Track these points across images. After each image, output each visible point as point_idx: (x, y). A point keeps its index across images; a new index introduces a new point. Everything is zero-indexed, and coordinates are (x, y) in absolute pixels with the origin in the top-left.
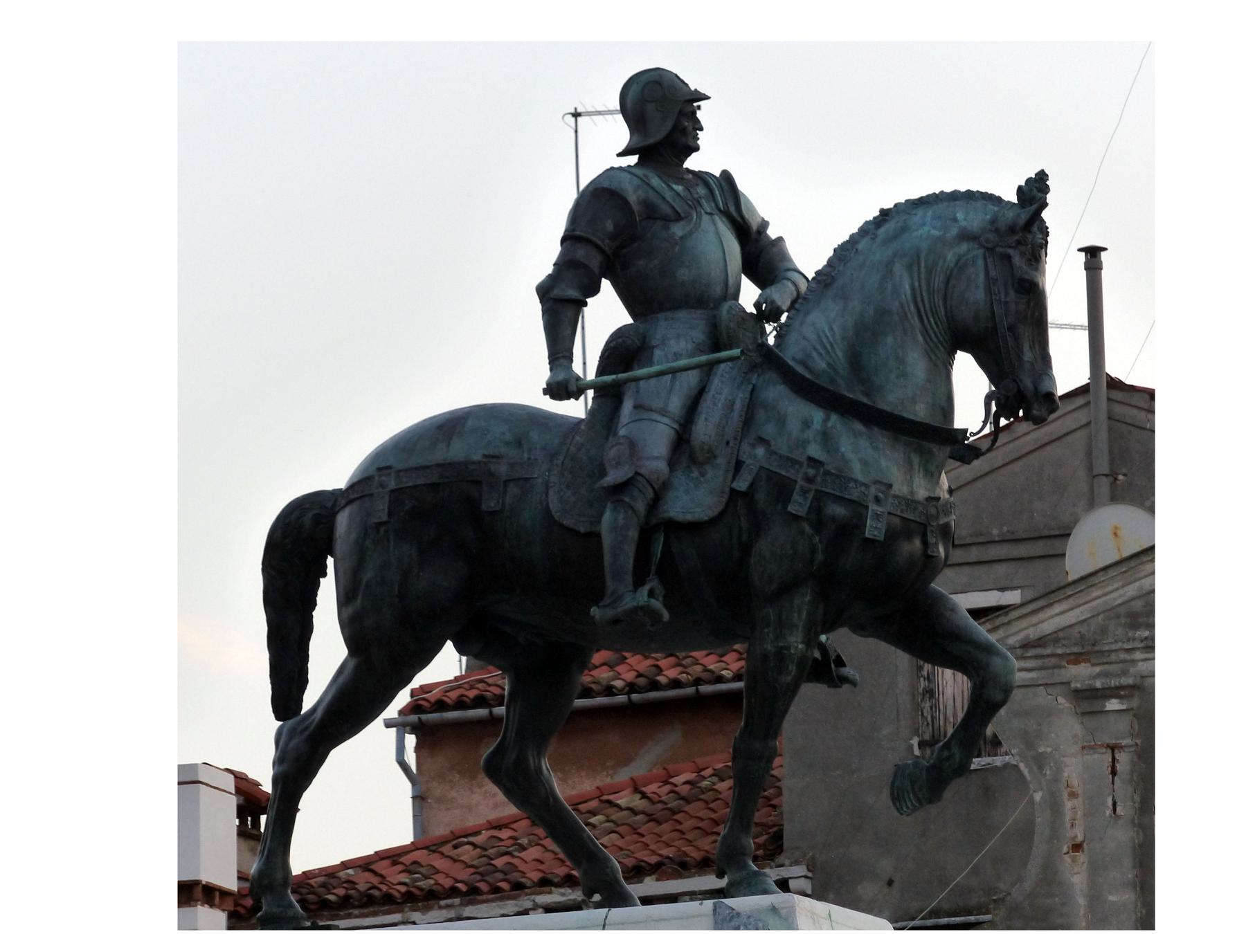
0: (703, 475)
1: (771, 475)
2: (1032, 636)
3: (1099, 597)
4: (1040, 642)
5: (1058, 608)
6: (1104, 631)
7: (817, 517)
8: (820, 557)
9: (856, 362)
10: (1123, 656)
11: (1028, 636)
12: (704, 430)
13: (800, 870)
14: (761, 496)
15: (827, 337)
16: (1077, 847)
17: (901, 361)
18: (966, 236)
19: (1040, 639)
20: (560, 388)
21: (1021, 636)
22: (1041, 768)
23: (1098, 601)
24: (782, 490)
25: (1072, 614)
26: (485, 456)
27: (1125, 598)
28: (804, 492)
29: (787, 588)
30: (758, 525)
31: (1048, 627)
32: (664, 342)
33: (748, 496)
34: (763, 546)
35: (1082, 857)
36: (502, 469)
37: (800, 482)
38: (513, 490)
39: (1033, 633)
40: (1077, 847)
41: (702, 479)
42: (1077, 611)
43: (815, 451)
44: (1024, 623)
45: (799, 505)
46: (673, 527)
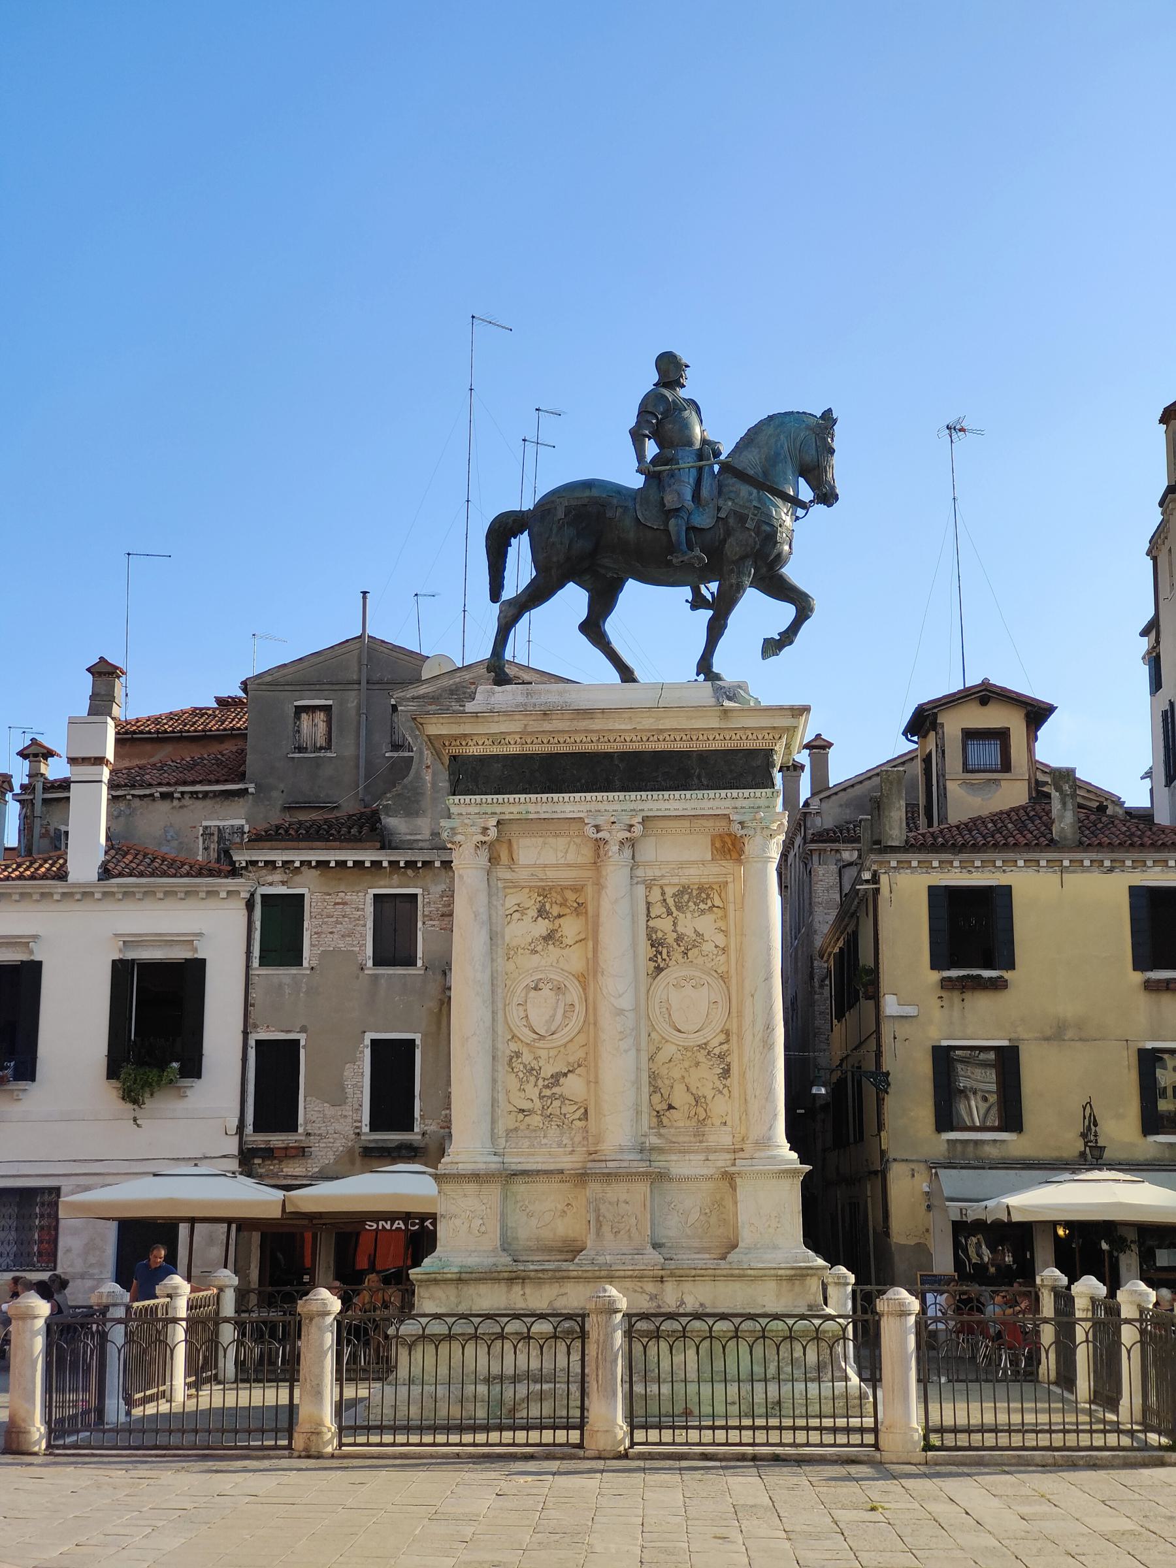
0: (704, 510)
1: (735, 512)
4: (418, 697)
6: (441, 695)
7: (758, 530)
8: (758, 546)
9: (765, 474)
10: (448, 703)
12: (705, 493)
13: (253, 785)
14: (731, 521)
16: (428, 767)
17: (785, 473)
18: (808, 428)
22: (416, 739)
24: (742, 519)
28: (752, 520)
29: (743, 558)
30: (728, 533)
31: (421, 692)
32: (682, 458)
33: (724, 520)
34: (731, 540)
35: (430, 771)
36: (615, 501)
37: (751, 516)
38: (620, 510)
40: (428, 767)
45: (750, 524)
46: (695, 529)
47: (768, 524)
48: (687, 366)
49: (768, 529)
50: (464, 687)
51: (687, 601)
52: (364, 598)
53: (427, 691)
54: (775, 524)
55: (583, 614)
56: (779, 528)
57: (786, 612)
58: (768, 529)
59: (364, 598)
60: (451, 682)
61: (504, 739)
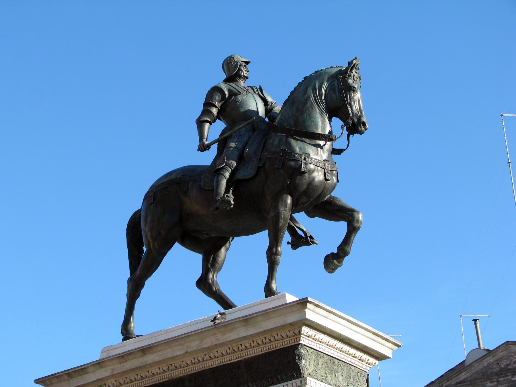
2: (458, 381)
3: (473, 370)
5: (464, 373)
11: (457, 382)
15: (287, 116)
19: (460, 382)
20: (203, 148)
21: (455, 382)
23: (474, 370)
25: (467, 375)
26: (182, 175)
27: (480, 369)
31: (462, 379)
39: (458, 381)
41: (249, 166)
42: (468, 374)
43: (283, 147)
44: (456, 378)
47: (292, 160)
48: (247, 63)
49: (292, 163)
50: (491, 368)
51: (288, 243)
52: (476, 324)
53: (465, 377)
54: (297, 157)
55: (198, 273)
56: (303, 161)
57: (342, 227)
58: (292, 163)
59: (476, 324)
60: (481, 367)
61: (105, 384)
